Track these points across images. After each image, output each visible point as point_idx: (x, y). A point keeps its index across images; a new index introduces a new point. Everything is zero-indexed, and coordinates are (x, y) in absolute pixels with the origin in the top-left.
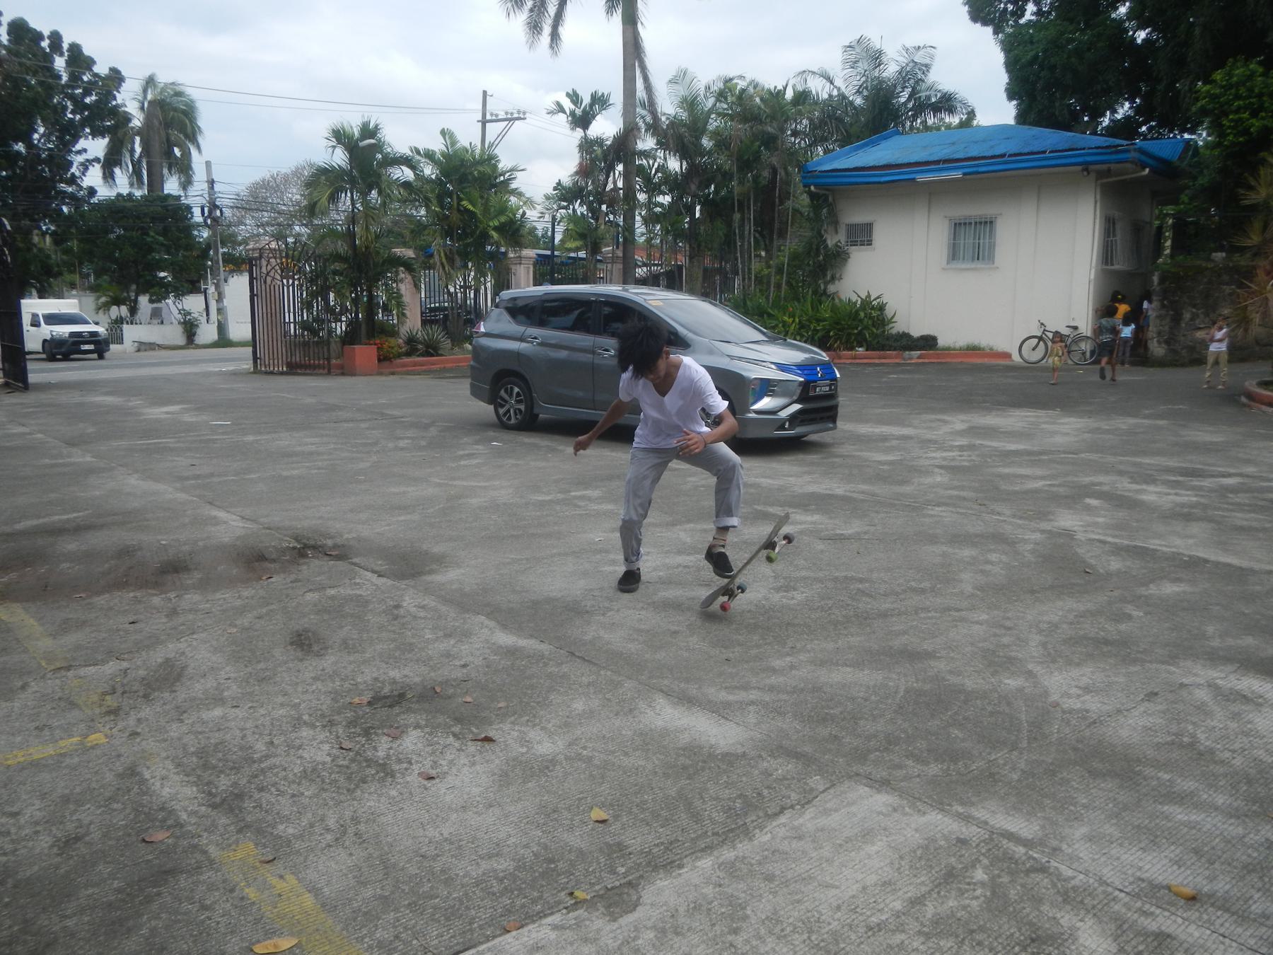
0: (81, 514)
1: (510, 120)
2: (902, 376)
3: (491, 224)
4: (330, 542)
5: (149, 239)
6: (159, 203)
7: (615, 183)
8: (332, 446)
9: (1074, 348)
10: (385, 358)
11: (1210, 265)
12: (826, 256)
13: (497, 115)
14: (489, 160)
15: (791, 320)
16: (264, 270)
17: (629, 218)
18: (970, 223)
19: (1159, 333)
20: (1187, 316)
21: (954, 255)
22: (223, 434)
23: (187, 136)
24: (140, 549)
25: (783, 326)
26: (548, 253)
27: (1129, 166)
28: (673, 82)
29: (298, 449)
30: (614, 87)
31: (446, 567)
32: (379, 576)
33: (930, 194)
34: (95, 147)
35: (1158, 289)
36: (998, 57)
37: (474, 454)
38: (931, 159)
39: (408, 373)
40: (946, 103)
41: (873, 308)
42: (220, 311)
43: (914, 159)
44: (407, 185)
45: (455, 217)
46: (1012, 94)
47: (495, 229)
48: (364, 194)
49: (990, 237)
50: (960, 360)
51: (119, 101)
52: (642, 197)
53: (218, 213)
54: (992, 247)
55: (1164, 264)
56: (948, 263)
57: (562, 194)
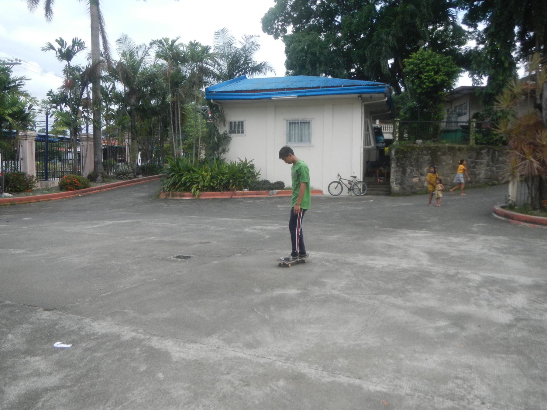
3: (6, 112)
7: (88, 94)
9: (355, 187)
11: (418, 146)
15: (206, 174)
17: (97, 114)
18: (298, 123)
19: (396, 179)
20: (409, 171)
25: (202, 177)
26: (45, 134)
27: (382, 95)
28: (120, 41)
30: (87, 38)
33: (276, 107)
35: (394, 157)
38: (279, 87)
47: (10, 115)
52: (104, 104)
54: (310, 135)
55: (397, 145)
57: (53, 99)
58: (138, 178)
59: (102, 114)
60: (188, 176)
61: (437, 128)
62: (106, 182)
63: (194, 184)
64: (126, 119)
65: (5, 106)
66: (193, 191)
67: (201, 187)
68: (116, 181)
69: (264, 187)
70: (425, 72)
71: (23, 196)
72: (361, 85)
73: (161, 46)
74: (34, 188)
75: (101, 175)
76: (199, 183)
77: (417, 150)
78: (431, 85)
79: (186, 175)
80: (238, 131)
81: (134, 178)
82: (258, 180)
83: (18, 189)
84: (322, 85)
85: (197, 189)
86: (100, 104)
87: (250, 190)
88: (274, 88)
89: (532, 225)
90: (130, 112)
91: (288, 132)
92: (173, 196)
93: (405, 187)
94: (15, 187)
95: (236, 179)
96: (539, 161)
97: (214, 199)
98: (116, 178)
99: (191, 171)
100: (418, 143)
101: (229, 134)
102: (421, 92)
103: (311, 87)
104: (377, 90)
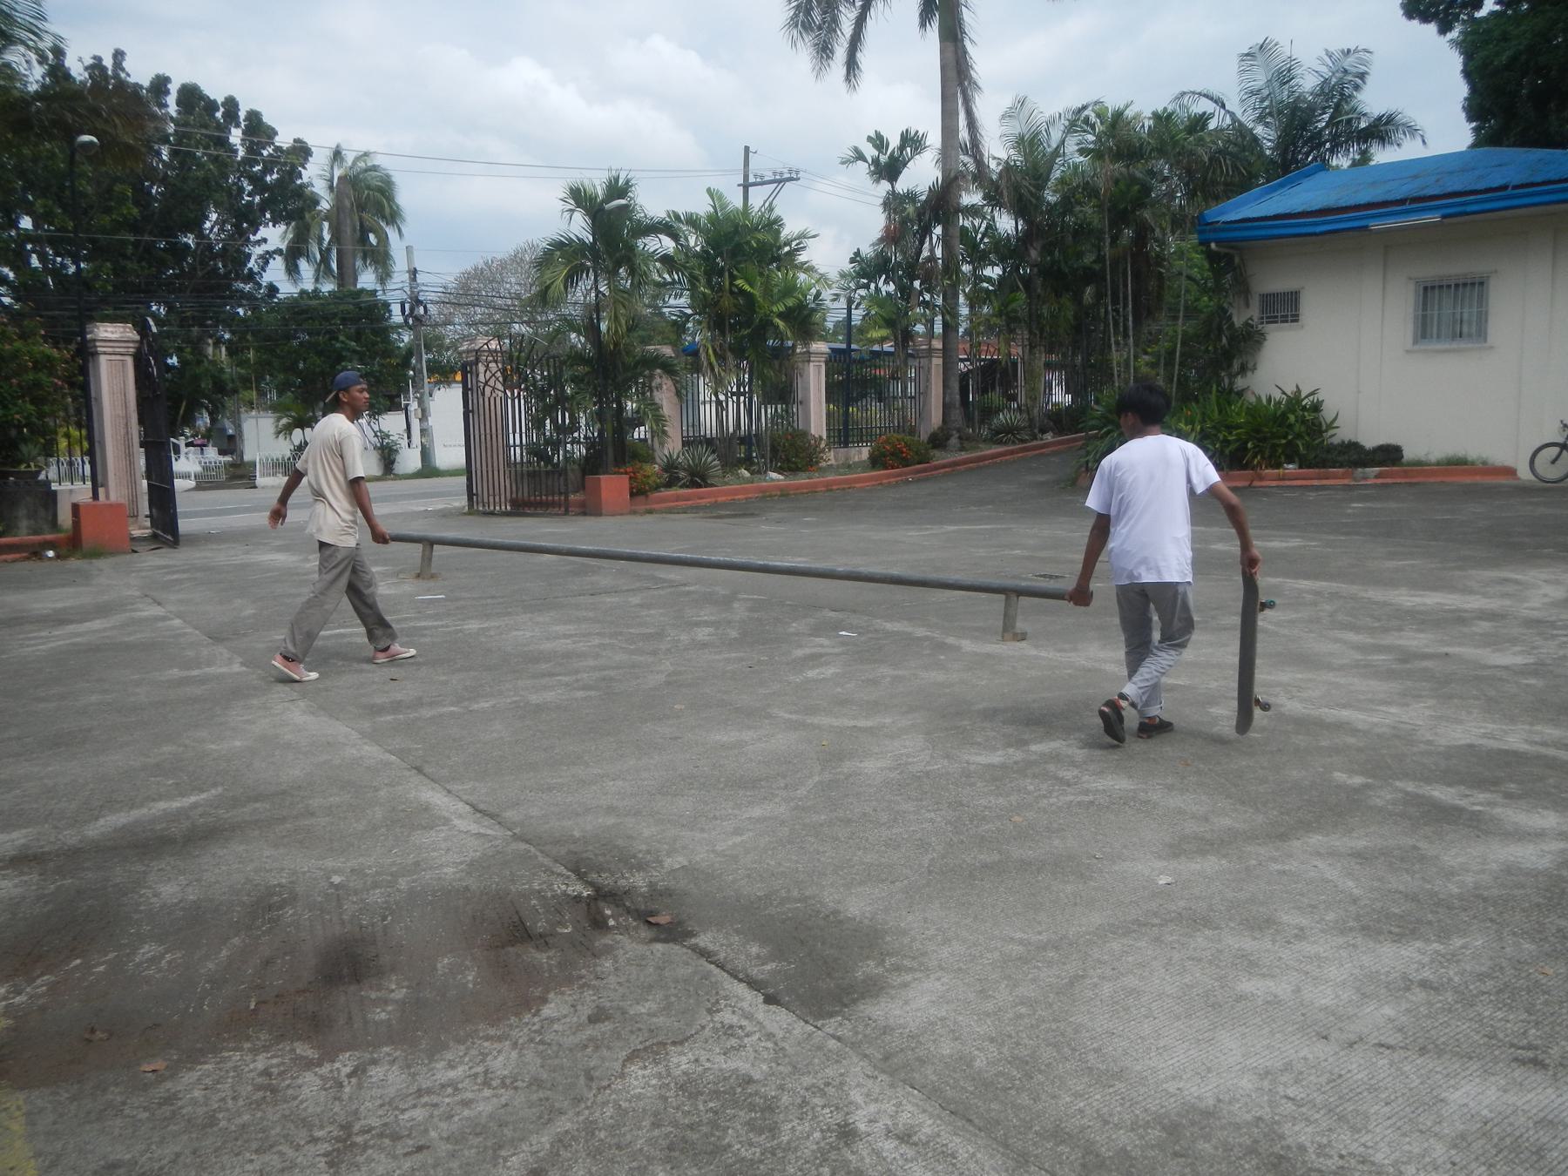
0: (204, 796)
1: (779, 182)
2: (1368, 505)
3: (775, 309)
4: (639, 881)
5: (338, 345)
6: (351, 300)
7: (932, 250)
8: (597, 642)
10: (638, 492)
12: (1231, 339)
13: (762, 177)
14: (773, 225)
15: (1189, 427)
16: (482, 378)
18: (1449, 286)
21: (1424, 331)
22: (436, 617)
23: (384, 217)
24: (293, 899)
26: (844, 346)
28: (1007, 116)
29: (547, 646)
31: (898, 969)
32: (770, 1000)
34: (274, 235)
36: (1456, 61)
37: (821, 655)
39: (670, 511)
40: (1382, 130)
41: (1304, 408)
42: (423, 432)
43: (1364, 197)
44: (667, 260)
45: (727, 302)
46: (1475, 110)
47: (781, 315)
48: (613, 273)
51: (305, 179)
52: (966, 268)
53: (421, 311)
56: (1415, 342)
57: (861, 269)
58: (1042, 439)
59: (964, 291)
62: (967, 450)
64: (1014, 300)
65: (772, 297)
68: (990, 449)
69: (1340, 459)
71: (802, 480)
74: (823, 464)
75: (957, 435)
80: (1282, 316)
81: (1032, 440)
82: (1330, 441)
83: (793, 466)
84: (1517, 181)
86: (958, 270)
87: (1300, 467)
88: (1380, 199)
90: (1027, 282)
91: (1420, 312)
94: (789, 461)
95: (1264, 439)
98: (991, 439)
101: (1260, 327)
103: (1483, 188)
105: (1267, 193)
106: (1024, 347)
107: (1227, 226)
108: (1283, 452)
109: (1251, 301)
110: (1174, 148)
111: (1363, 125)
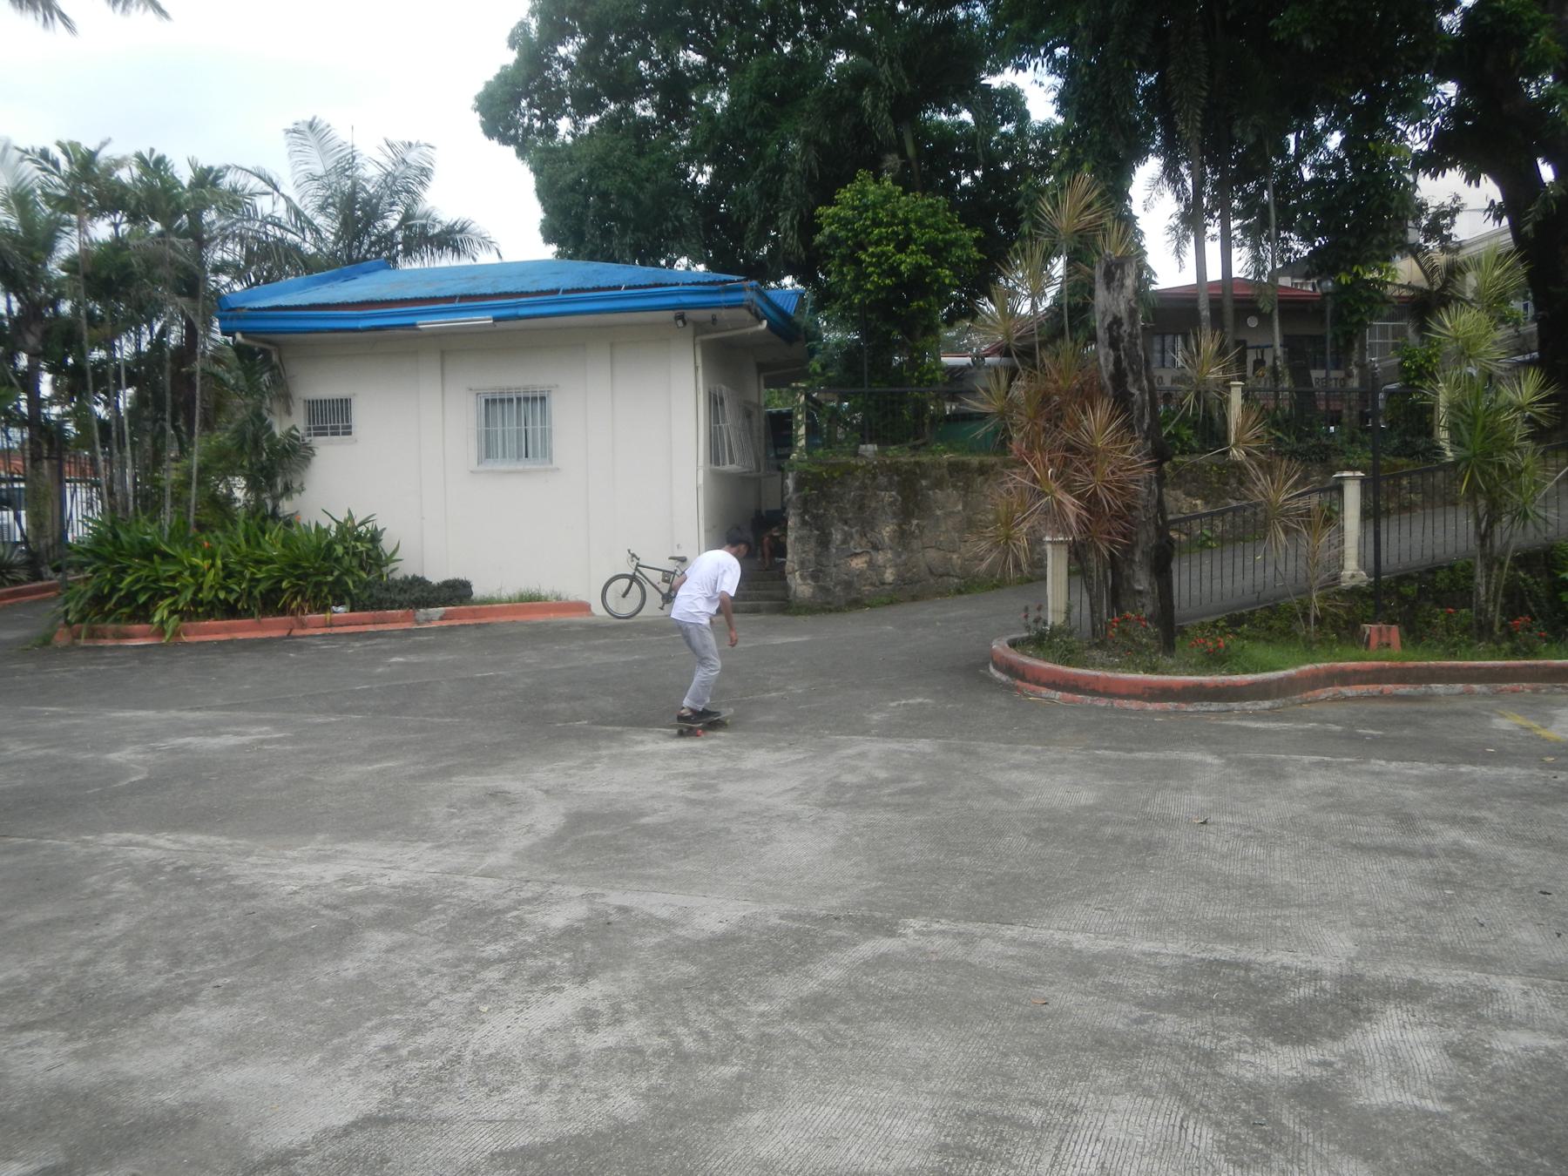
2: (413, 658)
11: (862, 463)
12: (272, 451)
15: (207, 563)
18: (510, 400)
19: (802, 564)
20: (837, 536)
21: (488, 449)
25: (193, 575)
27: (744, 313)
33: (443, 353)
35: (794, 498)
38: (441, 294)
41: (359, 538)
46: (550, 233)
49: (543, 422)
50: (511, 618)
54: (546, 436)
60: (144, 573)
61: (920, 409)
63: (163, 597)
66: (157, 619)
67: (186, 604)
70: (871, 244)
72: (677, 284)
73: (50, 167)
76: (175, 592)
77: (858, 473)
78: (888, 281)
79: (137, 570)
80: (332, 428)
82: (391, 576)
85: (172, 613)
87: (352, 610)
89: (1070, 696)
92: (92, 635)
93: (831, 585)
96: (1079, 497)
97: (231, 642)
99: (156, 557)
100: (867, 454)
102: (862, 301)
104: (722, 298)
105: (315, 285)
106: (24, 460)
107: (254, 313)
108: (330, 592)
109: (293, 409)
110: (169, 204)
111: (437, 230)
